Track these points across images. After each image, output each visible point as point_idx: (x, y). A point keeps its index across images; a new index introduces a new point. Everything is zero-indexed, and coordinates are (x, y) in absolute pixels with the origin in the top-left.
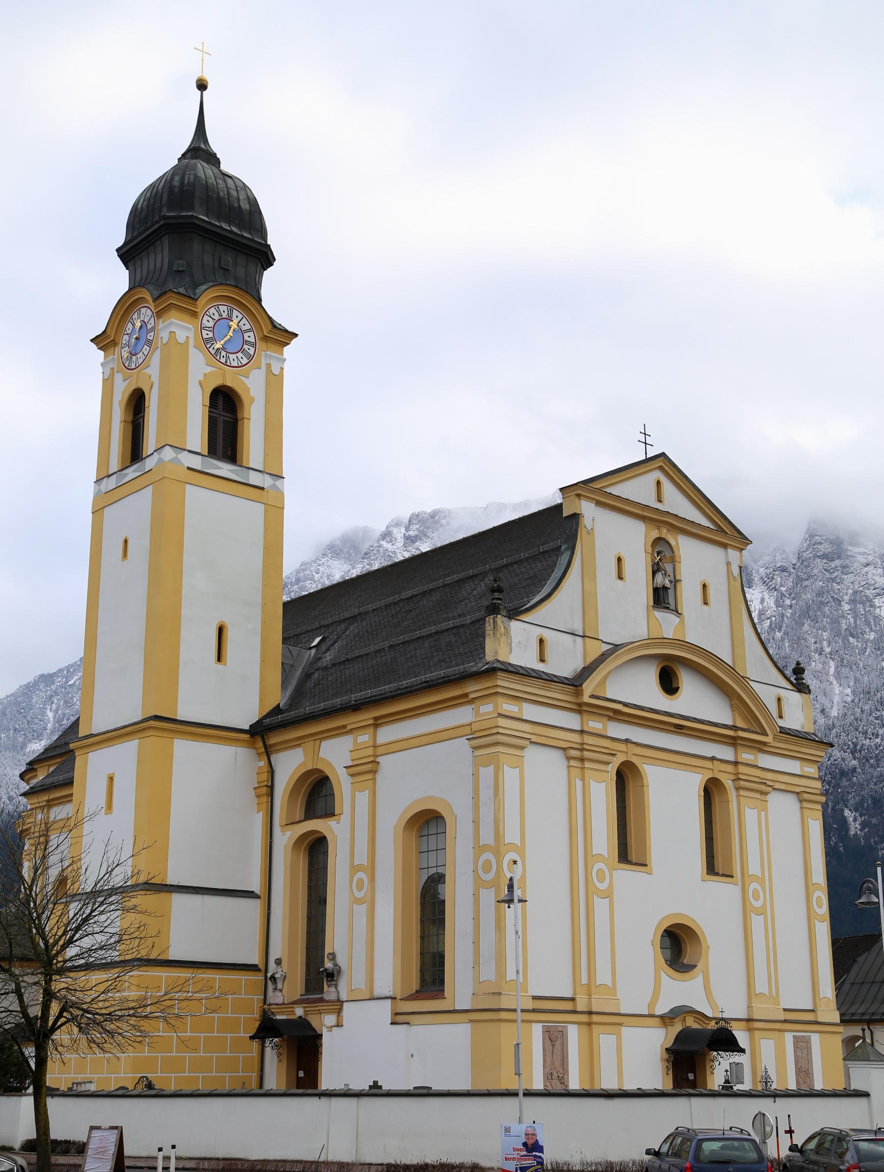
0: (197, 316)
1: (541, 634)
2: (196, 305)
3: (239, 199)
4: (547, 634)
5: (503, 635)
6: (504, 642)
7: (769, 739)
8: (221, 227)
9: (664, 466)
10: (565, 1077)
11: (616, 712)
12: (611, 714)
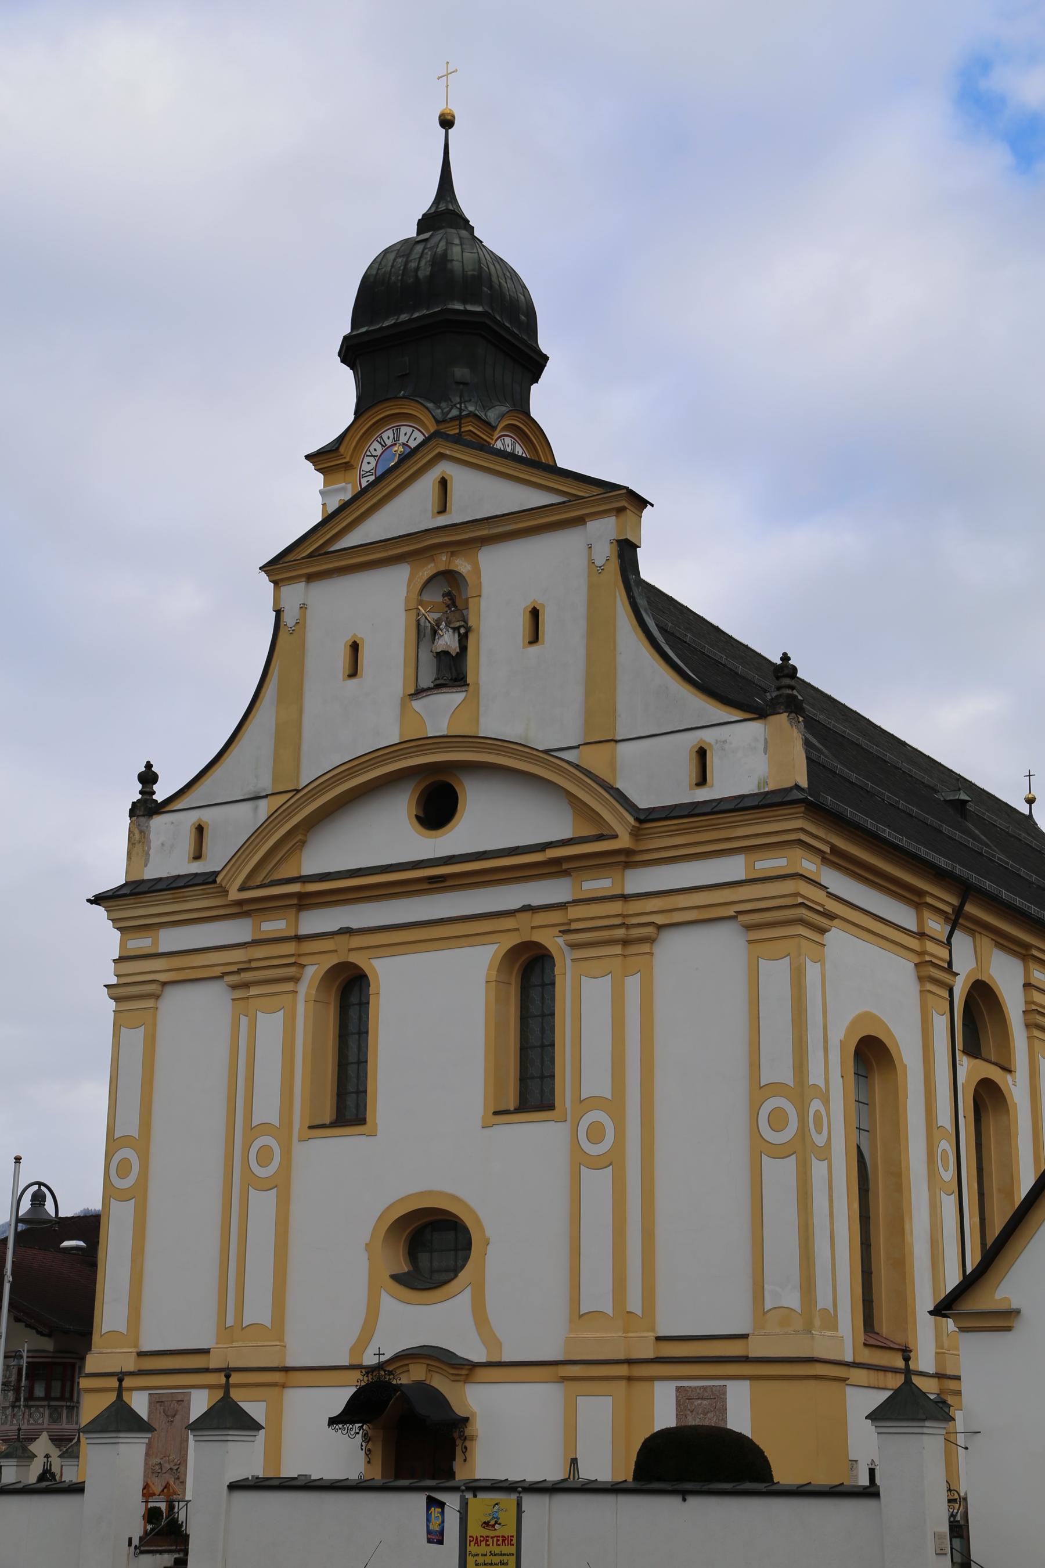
0: (352, 466)
1: (200, 819)
2: (342, 455)
3: (418, 269)
4: (206, 816)
5: (137, 844)
6: (138, 854)
7: (624, 841)
8: (382, 328)
9: (443, 451)
10: (182, 1469)
11: (300, 896)
12: (295, 901)
